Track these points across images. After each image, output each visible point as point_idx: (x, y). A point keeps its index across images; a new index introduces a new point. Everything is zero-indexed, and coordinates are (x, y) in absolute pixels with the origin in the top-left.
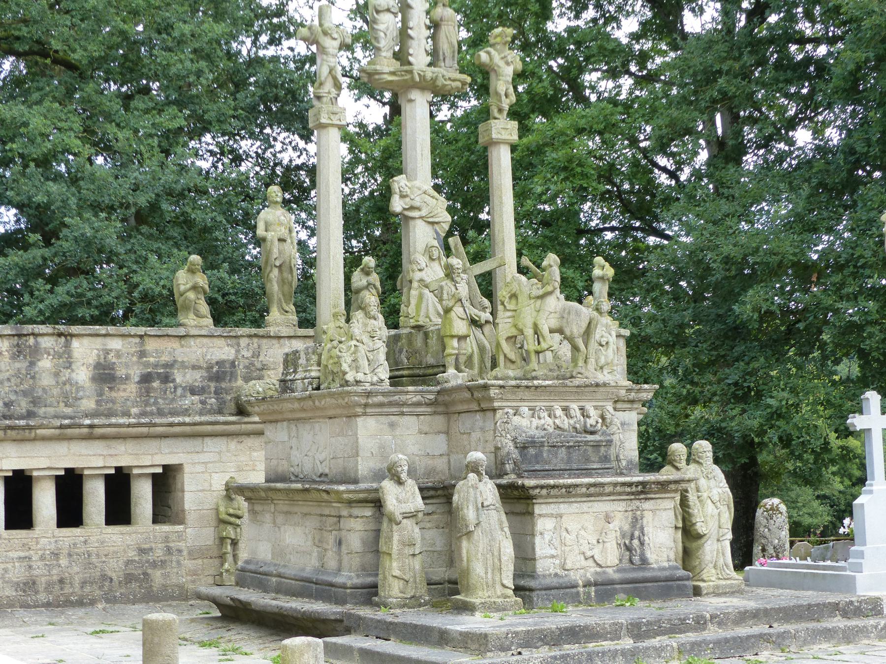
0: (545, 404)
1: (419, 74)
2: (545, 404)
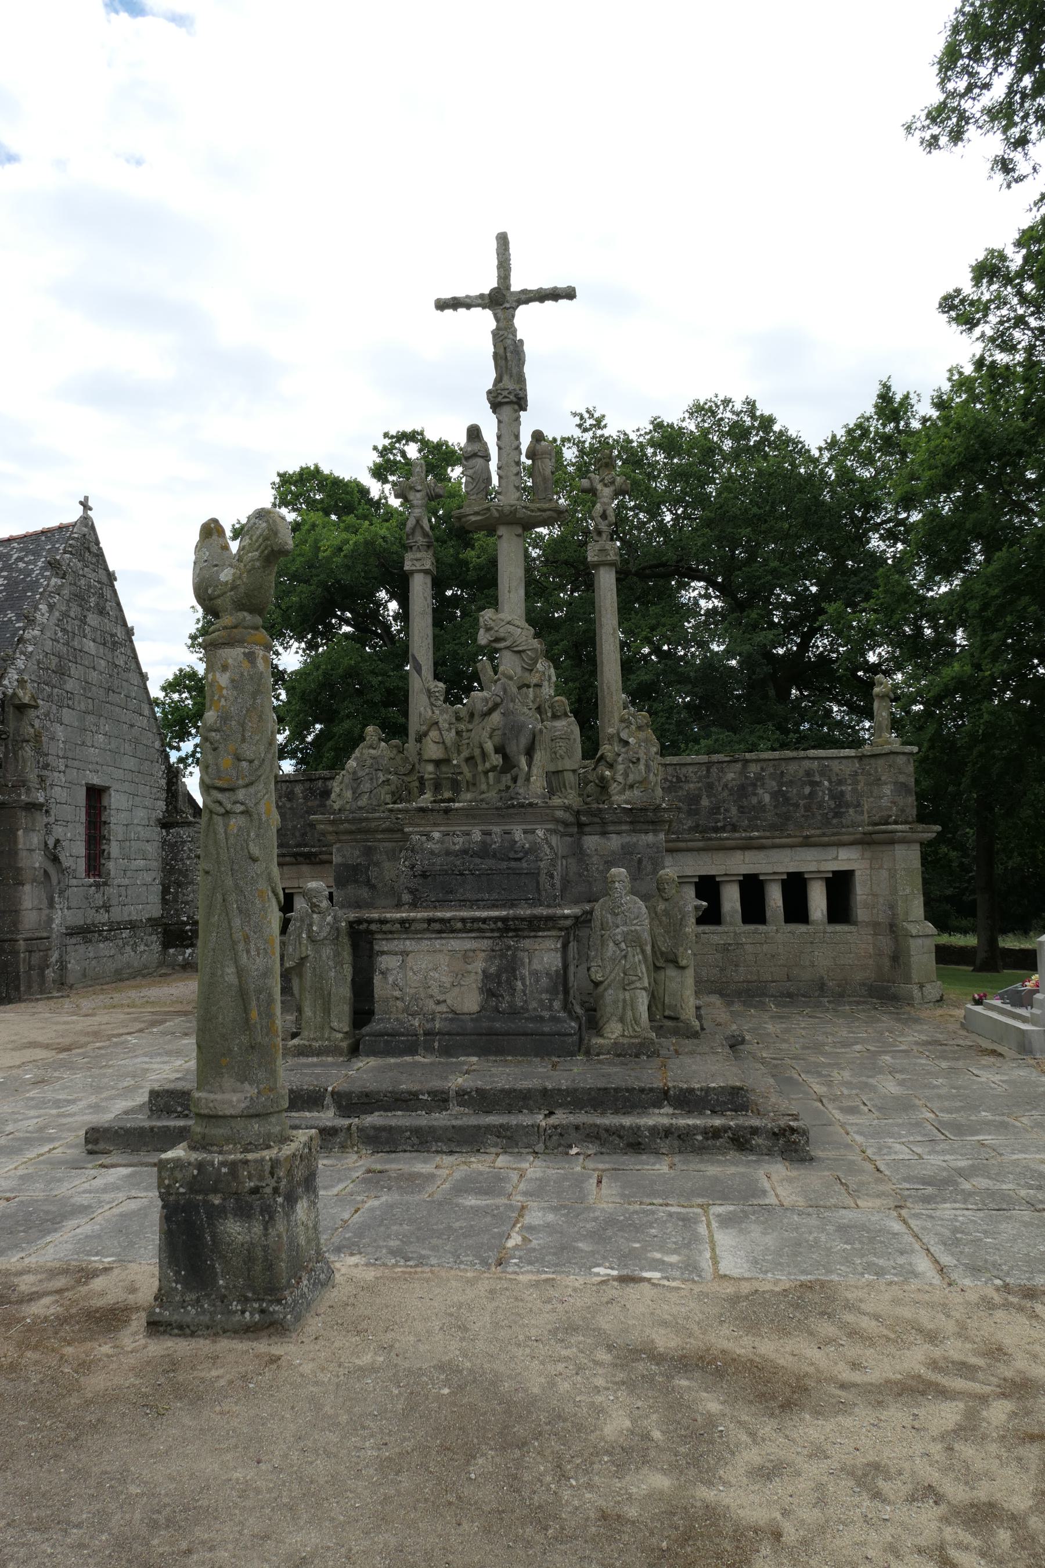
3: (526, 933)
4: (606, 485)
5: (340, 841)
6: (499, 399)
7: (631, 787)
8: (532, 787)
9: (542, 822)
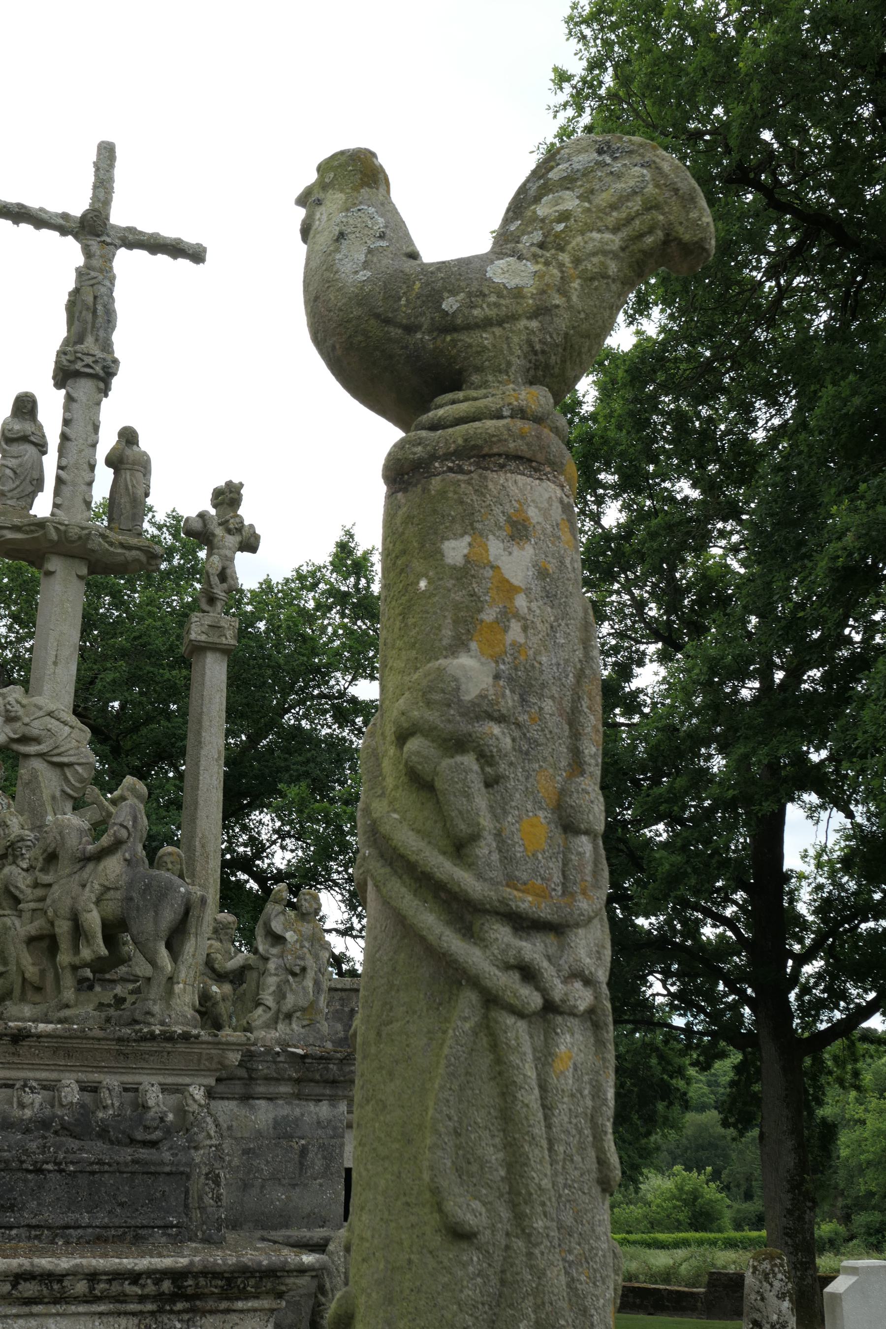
0: (44, 1075)
1: (56, 529)
2: (44, 1075)
3: (211, 1304)
4: (229, 531)
6: (79, 366)
7: (289, 1016)
8: (176, 1002)
9: (198, 1072)
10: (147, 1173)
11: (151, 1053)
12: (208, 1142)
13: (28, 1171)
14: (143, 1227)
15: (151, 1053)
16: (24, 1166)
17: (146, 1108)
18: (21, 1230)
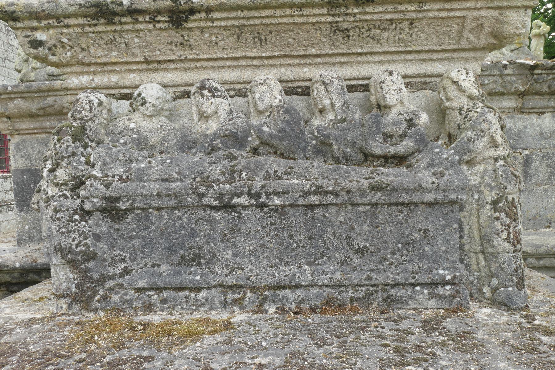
5: (18, 132)
9: (456, 52)
10: (397, 204)
11: (383, 25)
12: (492, 153)
13: (212, 208)
14: (396, 285)
15: (383, 25)
16: (205, 201)
17: (382, 107)
18: (214, 292)
